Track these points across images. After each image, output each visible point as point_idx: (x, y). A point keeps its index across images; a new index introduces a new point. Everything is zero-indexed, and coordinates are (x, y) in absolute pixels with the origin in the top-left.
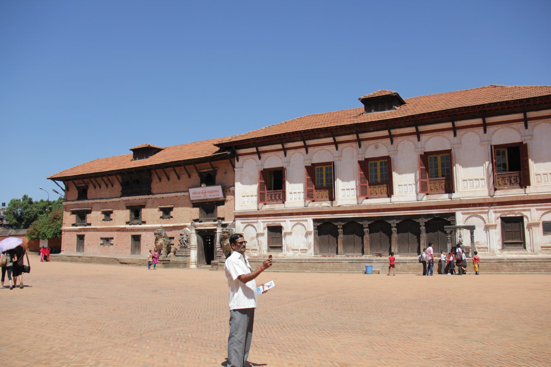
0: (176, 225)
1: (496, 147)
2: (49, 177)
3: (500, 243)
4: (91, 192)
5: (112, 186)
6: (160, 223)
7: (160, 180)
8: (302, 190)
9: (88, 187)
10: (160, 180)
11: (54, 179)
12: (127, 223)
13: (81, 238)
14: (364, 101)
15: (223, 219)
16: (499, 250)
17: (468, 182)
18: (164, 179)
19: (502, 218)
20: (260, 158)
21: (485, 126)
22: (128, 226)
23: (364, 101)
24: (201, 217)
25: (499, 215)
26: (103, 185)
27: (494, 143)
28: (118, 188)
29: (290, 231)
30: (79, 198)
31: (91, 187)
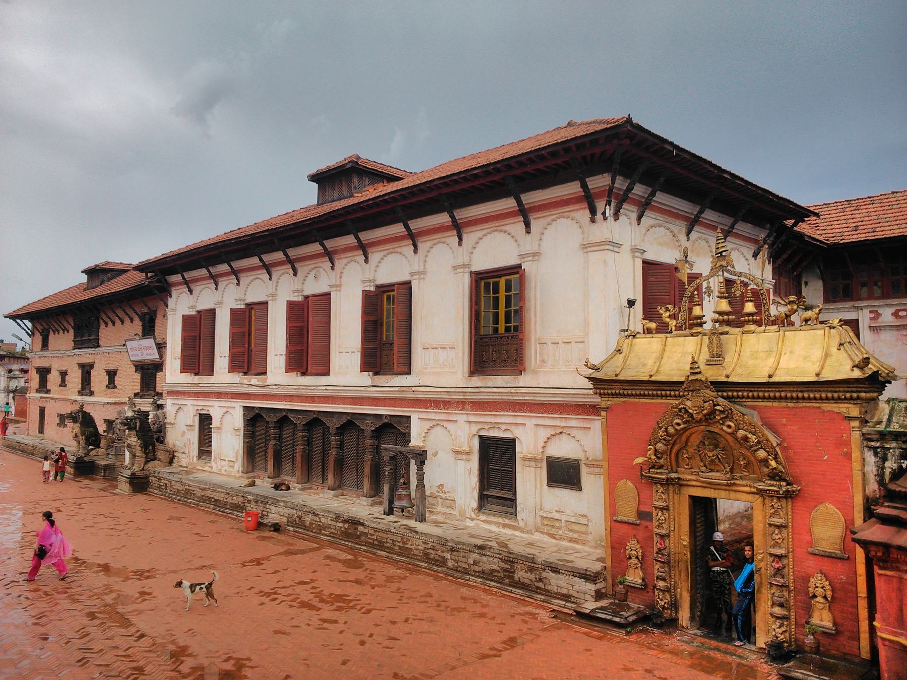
0: (117, 400)
1: (477, 273)
2: (7, 313)
3: (476, 494)
4: (52, 337)
5: (68, 332)
6: (106, 396)
7: (106, 324)
8: (227, 355)
9: (49, 332)
10: (106, 324)
11: (14, 317)
12: (81, 393)
13: (42, 411)
14: (314, 178)
15: (160, 395)
16: (473, 510)
17: (432, 351)
18: (110, 324)
19: (481, 438)
20: (191, 291)
21: (458, 228)
22: (79, 398)
23: (314, 178)
24: (142, 390)
25: (474, 429)
26: (61, 332)
27: (476, 268)
28: (72, 332)
29: (219, 425)
30: (42, 350)
31: (51, 333)
